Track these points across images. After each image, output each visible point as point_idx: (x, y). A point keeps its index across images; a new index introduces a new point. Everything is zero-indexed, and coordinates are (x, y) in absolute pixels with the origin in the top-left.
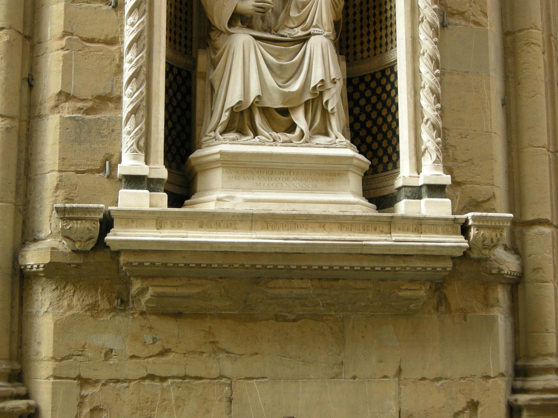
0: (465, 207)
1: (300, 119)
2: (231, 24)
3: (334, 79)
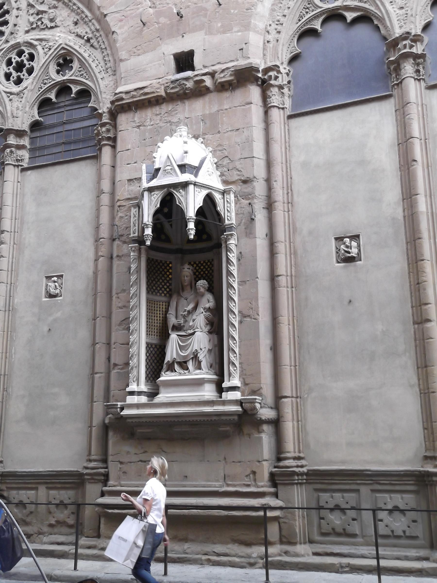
1: (190, 365)
2: (173, 330)
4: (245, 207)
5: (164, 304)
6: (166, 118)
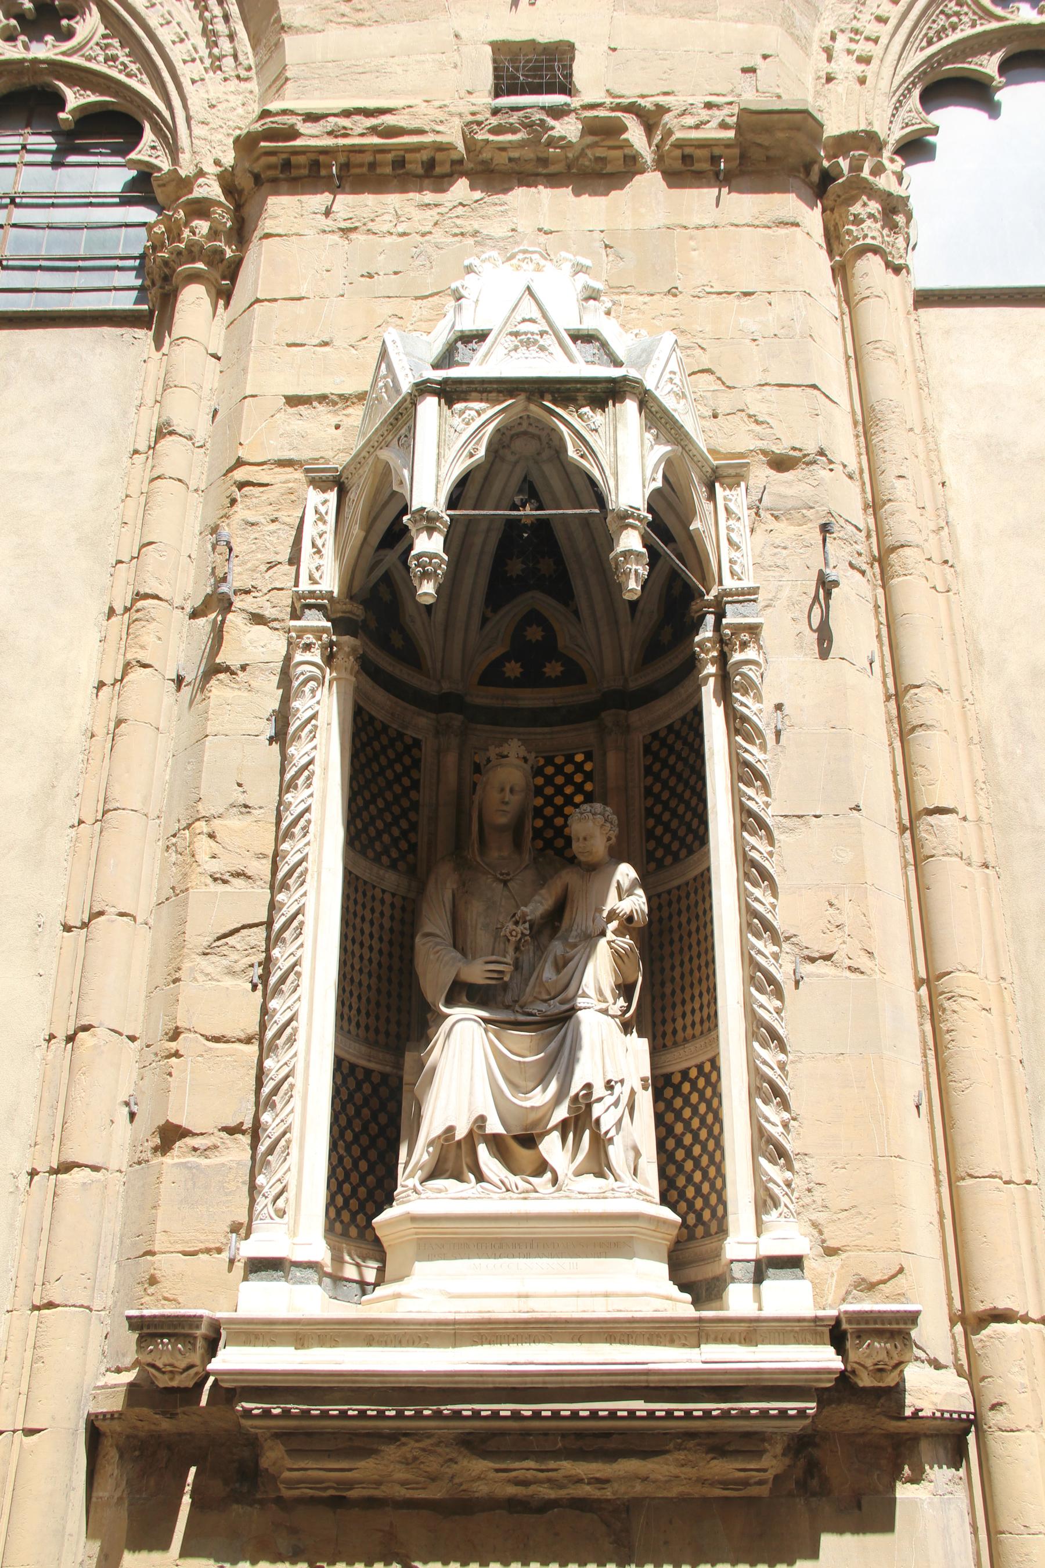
0: (848, 1293)
3: (609, 1082)
4: (788, 543)
5: (388, 898)
6: (458, 222)
